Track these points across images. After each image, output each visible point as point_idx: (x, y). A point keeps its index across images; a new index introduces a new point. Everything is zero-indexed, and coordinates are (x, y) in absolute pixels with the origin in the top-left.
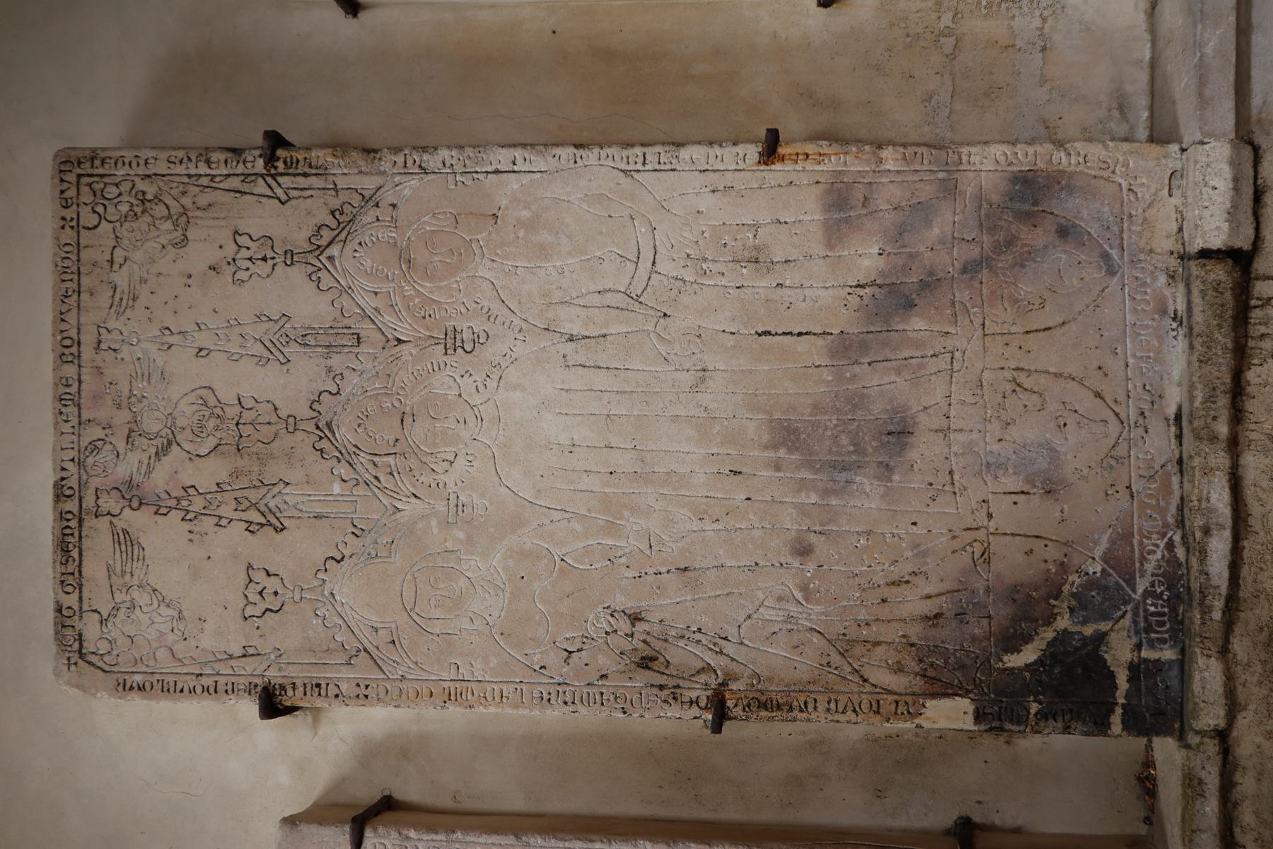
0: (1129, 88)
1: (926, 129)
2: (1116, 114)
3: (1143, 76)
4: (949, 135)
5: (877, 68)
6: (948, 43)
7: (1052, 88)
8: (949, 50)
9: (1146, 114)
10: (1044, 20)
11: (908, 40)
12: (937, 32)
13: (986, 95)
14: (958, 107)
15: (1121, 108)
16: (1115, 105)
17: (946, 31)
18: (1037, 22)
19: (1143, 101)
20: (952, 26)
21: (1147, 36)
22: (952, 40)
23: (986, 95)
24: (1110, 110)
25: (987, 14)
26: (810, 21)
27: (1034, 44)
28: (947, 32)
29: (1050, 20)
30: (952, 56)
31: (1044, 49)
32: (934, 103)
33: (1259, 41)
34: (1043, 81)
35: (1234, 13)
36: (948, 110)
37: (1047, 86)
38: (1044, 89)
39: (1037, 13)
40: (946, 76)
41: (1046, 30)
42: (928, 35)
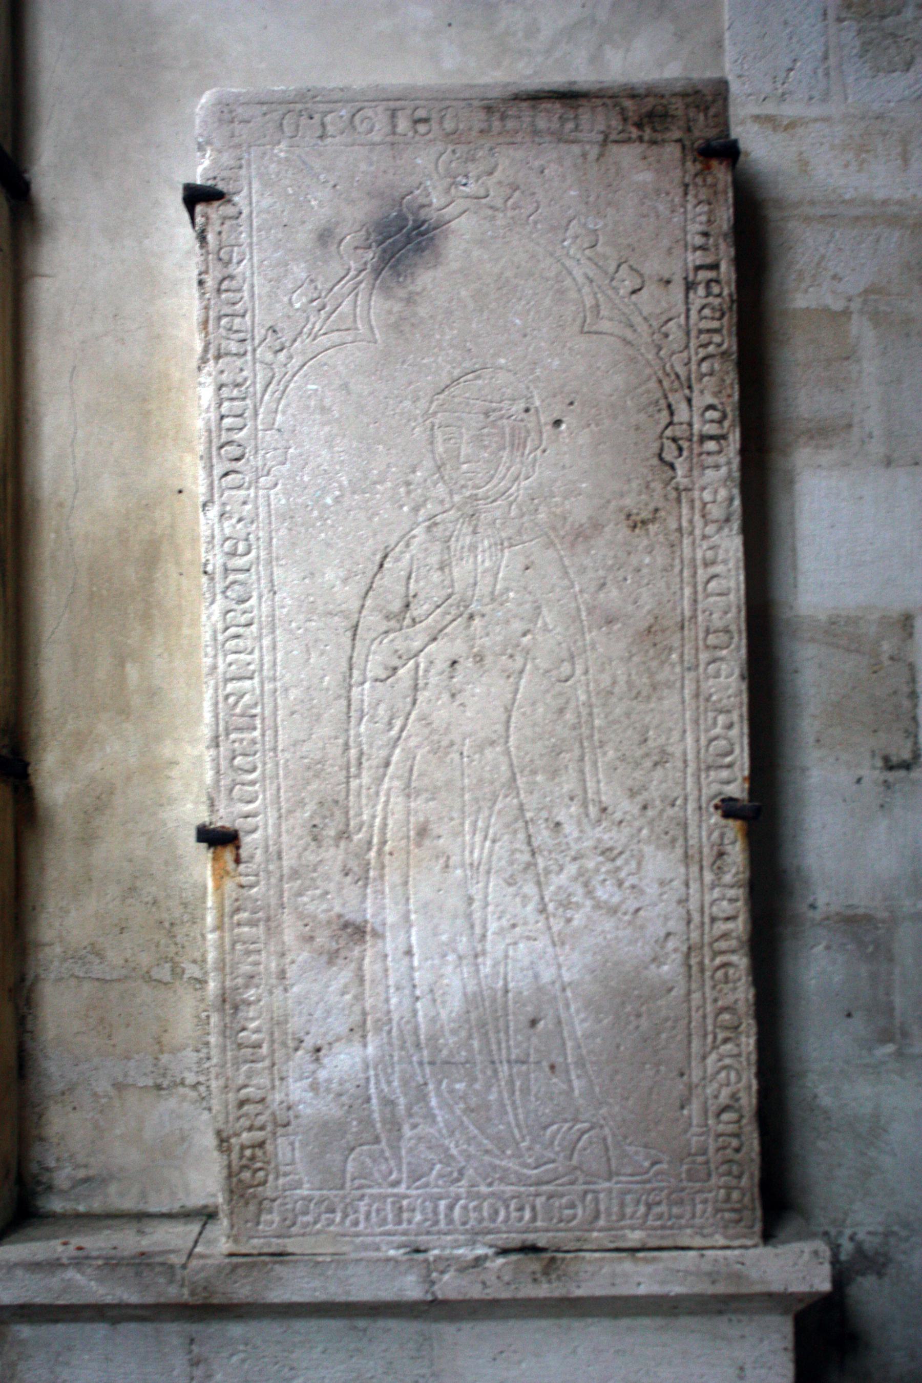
0: (113, 1189)
1: (58, 949)
2: (81, 1174)
3: (129, 1204)
4: (52, 976)
5: (132, 889)
6: (164, 973)
7: (110, 1098)
8: (156, 974)
9: (82, 1208)
10: (195, 1086)
11: (167, 925)
12: (177, 959)
13: (102, 1020)
14: (87, 986)
15: (87, 1180)
16: (91, 1172)
17: (179, 970)
18: (191, 1078)
19: (96, 1205)
20: (186, 976)
21: (176, 1207)
22: (167, 977)
23: (102, 1020)
24: (86, 1166)
25: (198, 1017)
26: (190, 806)
27: (164, 1075)
28: (177, 972)
29: (193, 1094)
30: (148, 978)
31: (159, 1087)
32: (91, 957)
33: (100, 1330)
34: (120, 1087)
35: (116, 1301)
36: (81, 974)
37: (112, 1092)
38: (109, 1088)
39: (202, 1079)
40: (124, 972)
41: (182, 1090)
42: (173, 949)
